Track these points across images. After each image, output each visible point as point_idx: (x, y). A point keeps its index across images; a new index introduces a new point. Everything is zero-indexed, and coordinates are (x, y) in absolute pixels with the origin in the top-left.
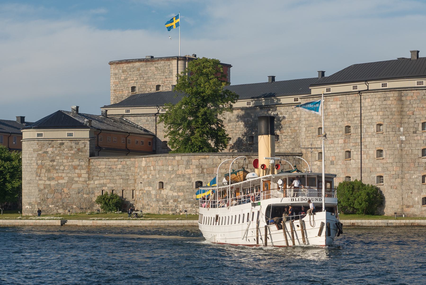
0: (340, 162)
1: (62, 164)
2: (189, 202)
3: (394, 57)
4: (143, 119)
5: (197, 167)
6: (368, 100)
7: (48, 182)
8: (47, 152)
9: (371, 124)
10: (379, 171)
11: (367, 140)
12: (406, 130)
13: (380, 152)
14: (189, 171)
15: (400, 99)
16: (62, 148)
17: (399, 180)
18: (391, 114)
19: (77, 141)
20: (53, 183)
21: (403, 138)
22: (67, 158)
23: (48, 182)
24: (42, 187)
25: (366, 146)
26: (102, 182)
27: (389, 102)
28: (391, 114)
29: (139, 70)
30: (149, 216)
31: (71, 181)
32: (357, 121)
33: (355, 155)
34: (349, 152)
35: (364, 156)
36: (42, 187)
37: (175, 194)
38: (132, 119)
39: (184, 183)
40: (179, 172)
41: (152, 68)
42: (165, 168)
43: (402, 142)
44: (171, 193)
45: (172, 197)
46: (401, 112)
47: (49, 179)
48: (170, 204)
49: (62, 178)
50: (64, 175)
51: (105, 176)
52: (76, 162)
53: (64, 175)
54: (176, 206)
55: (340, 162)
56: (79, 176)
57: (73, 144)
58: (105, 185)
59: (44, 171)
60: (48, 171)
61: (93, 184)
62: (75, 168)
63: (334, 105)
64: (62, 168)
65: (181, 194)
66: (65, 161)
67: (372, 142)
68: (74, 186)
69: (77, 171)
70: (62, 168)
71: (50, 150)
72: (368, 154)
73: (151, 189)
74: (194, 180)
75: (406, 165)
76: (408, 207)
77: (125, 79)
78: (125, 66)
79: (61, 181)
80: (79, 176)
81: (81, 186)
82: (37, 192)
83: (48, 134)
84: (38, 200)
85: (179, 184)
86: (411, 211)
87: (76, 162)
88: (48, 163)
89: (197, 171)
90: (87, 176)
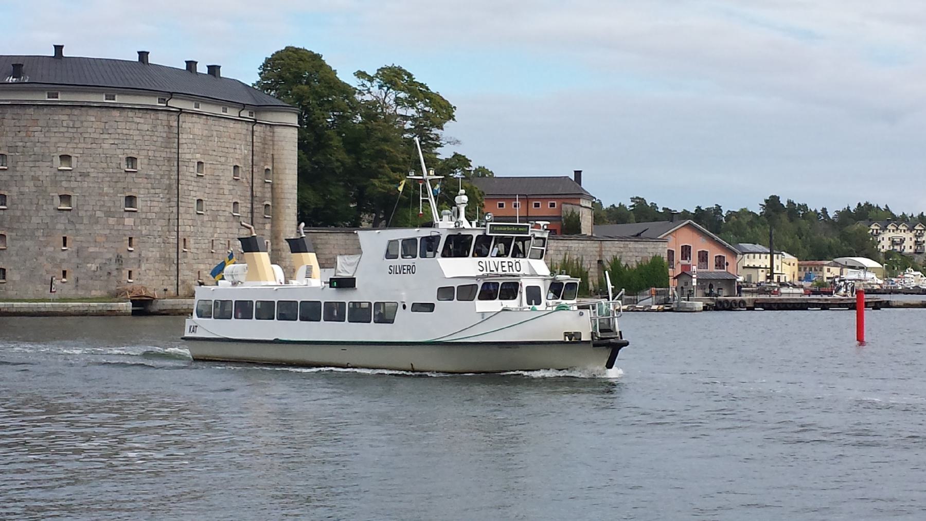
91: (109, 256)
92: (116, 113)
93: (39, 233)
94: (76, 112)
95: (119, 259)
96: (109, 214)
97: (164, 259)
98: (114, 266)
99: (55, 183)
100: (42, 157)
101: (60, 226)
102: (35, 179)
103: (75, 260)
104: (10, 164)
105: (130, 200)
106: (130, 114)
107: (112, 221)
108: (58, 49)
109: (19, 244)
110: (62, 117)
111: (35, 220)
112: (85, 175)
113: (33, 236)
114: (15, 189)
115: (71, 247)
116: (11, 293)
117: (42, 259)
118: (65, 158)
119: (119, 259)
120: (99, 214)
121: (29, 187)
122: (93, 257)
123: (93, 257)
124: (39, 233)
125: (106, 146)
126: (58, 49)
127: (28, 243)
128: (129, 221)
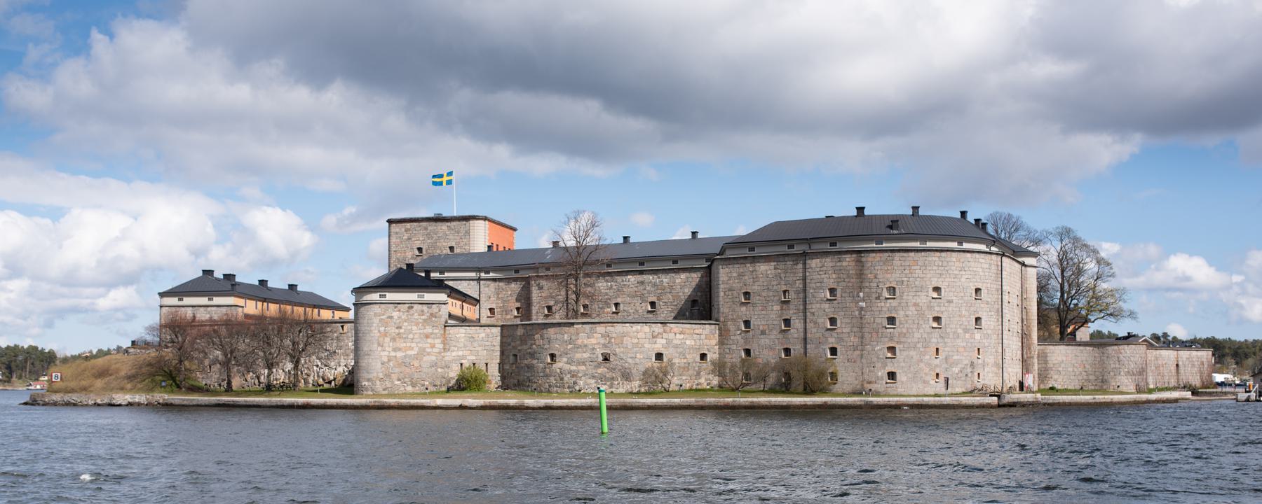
0: (775, 332)
1: (411, 331)
2: (594, 377)
3: (822, 215)
4: (465, 283)
5: (603, 336)
6: (814, 263)
7: (393, 354)
8: (391, 317)
9: (821, 288)
10: (832, 342)
11: (814, 307)
12: (868, 296)
13: (833, 321)
14: (593, 341)
15: (859, 261)
16: (411, 311)
17: (858, 352)
18: (848, 276)
19: (429, 304)
20: (399, 354)
21: (863, 304)
22: (417, 324)
23: (393, 354)
24: (385, 359)
25: (813, 314)
26: (461, 353)
27: (844, 264)
28: (848, 276)
29: (426, 229)
30: (1065, 391)
31: (422, 352)
32: (799, 284)
33: (797, 324)
34: (787, 322)
35: (809, 325)
36: (385, 359)
37: (573, 368)
38: (450, 283)
39: (586, 355)
40: (579, 342)
41: (443, 227)
42: (559, 336)
43: (862, 308)
44: (567, 367)
45: (570, 372)
46: (861, 275)
47: (395, 350)
48: (566, 379)
49: (411, 348)
50: (413, 345)
51: (465, 346)
52: (429, 330)
53: (413, 345)
54: (575, 383)
55: (775, 332)
56: (433, 346)
57: (425, 308)
58: (464, 357)
59: (387, 340)
60: (393, 340)
61: (449, 356)
62: (427, 336)
63: (763, 268)
64: (411, 336)
65: (583, 368)
66: (415, 328)
67: (820, 309)
68: (425, 359)
69: (429, 340)
70: (411, 336)
71: (396, 314)
72: (815, 323)
73: (535, 362)
74: (599, 351)
75: (867, 336)
76: (870, 383)
77: (409, 239)
78: (408, 225)
79: (410, 353)
80: (433, 346)
81: (434, 358)
82: (379, 365)
83: (392, 296)
84: (381, 376)
85: (578, 356)
86: (874, 387)
87: (429, 330)
88: (393, 330)
89: (602, 341)
90: (441, 346)
91: (966, 362)
92: (968, 255)
93: (919, 345)
94: (943, 254)
95: (972, 365)
96: (966, 331)
97: (996, 364)
98: (969, 370)
99: (930, 307)
100: (922, 289)
101: (934, 340)
102: (915, 305)
103: (945, 366)
104: (898, 294)
105: (978, 319)
106: (977, 255)
107: (967, 336)
108: (916, 209)
109: (905, 353)
110: (935, 257)
111: (917, 335)
112: (950, 302)
113: (915, 347)
114: (902, 313)
115: (942, 355)
116: (900, 391)
117: (922, 365)
118: (937, 289)
119: (972, 365)
120: (960, 331)
121: (912, 311)
122: (956, 363)
123: (956, 363)
124: (919, 345)
125: (963, 280)
126: (916, 209)
127: (912, 353)
128: (978, 336)
